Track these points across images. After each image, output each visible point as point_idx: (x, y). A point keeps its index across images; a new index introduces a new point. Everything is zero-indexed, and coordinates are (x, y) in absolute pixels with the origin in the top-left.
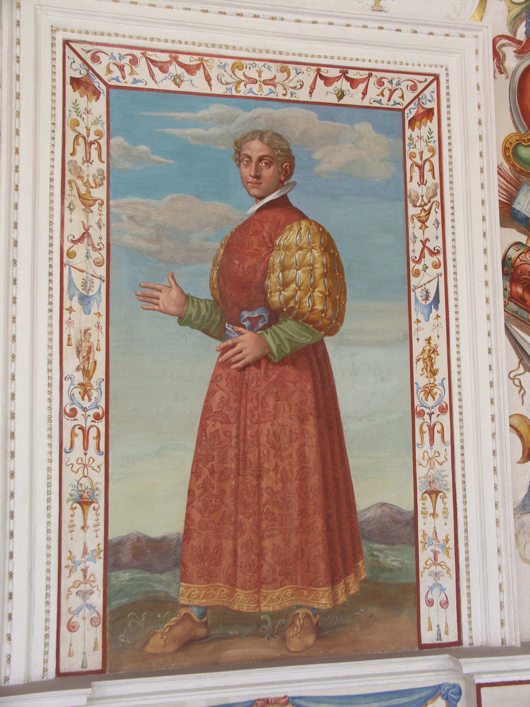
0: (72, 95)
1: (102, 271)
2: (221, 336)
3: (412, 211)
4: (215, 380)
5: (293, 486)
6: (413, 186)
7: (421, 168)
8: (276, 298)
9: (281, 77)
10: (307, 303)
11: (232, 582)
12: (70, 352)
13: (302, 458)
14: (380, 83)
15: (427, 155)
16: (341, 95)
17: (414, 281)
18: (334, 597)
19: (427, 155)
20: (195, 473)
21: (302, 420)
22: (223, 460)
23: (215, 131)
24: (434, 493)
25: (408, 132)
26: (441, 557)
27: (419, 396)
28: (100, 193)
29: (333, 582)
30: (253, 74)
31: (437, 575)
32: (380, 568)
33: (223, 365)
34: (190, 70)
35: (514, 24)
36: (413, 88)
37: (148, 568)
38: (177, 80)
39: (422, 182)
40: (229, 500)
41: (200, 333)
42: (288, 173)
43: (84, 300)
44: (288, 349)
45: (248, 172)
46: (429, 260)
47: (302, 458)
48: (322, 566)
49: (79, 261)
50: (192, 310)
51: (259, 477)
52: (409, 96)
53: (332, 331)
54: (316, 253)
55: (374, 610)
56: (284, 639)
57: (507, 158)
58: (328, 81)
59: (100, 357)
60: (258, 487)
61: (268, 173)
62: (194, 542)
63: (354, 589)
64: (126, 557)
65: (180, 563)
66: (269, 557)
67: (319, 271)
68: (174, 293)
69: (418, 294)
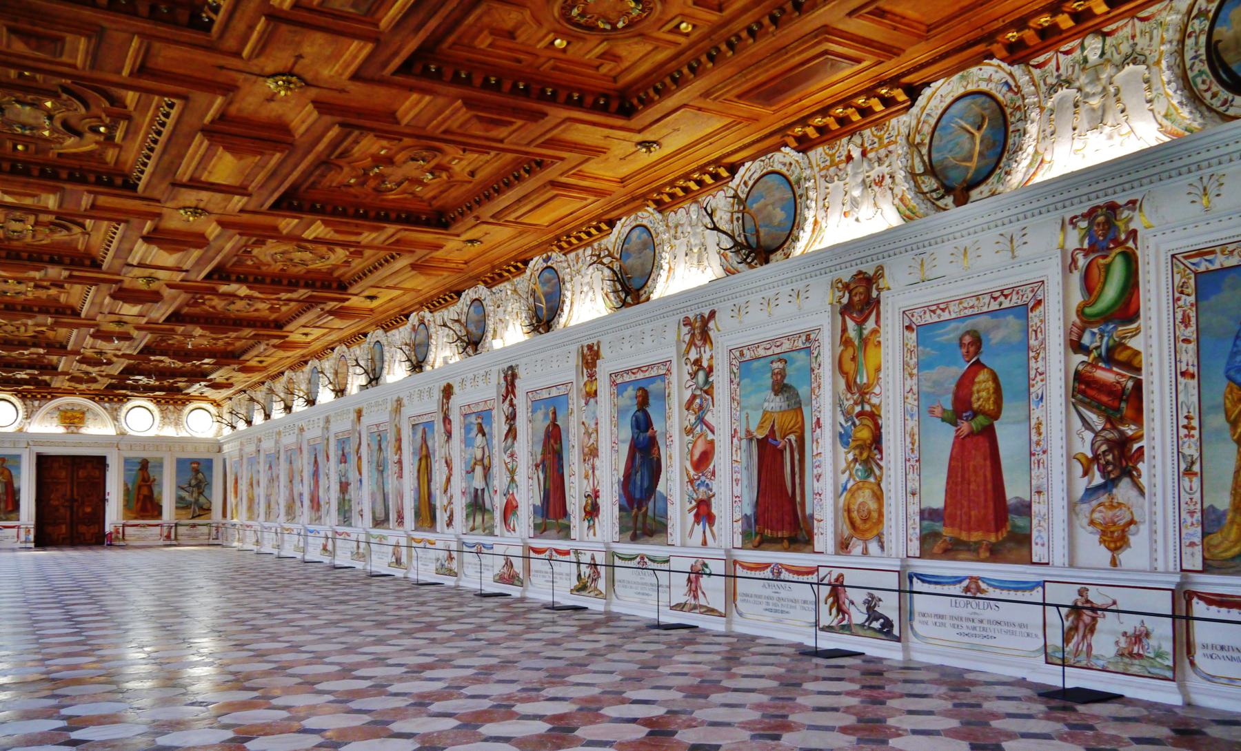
0: (906, 333)
1: (916, 403)
2: (955, 424)
3: (1032, 354)
4: (954, 444)
5: (981, 489)
6: (1032, 342)
7: (1036, 331)
8: (975, 406)
9: (976, 303)
10: (987, 407)
11: (961, 529)
12: (907, 436)
13: (985, 476)
14: (1018, 293)
15: (1039, 324)
16: (1001, 304)
17: (1032, 390)
18: (997, 538)
19: (1039, 324)
20: (948, 483)
21: (985, 460)
22: (957, 477)
23: (952, 336)
24: (1039, 492)
25: (1030, 314)
26: (1042, 523)
27: (1033, 446)
28: (915, 371)
29: (997, 530)
30: (965, 305)
31: (1039, 531)
32: (1014, 526)
33: (957, 437)
34: (943, 310)
35: (1082, 241)
36: (1032, 291)
37: (932, 520)
38: (939, 316)
39: (1036, 339)
40: (959, 494)
41: (948, 425)
42: (979, 348)
43: (912, 416)
44: (980, 428)
45: (964, 350)
46: (1039, 378)
47: (985, 476)
48: (993, 524)
49: (909, 400)
50: (946, 415)
51: (969, 484)
52: (1031, 295)
53: (996, 417)
54: (990, 383)
55: (1012, 545)
56: (978, 553)
57: (1078, 316)
58: (995, 299)
59: (916, 437)
60: (969, 489)
61: (972, 349)
62: (948, 511)
63: (1005, 535)
64: (926, 515)
65: (943, 519)
66: (973, 518)
67: (991, 391)
68: (940, 409)
69: (1033, 396)
